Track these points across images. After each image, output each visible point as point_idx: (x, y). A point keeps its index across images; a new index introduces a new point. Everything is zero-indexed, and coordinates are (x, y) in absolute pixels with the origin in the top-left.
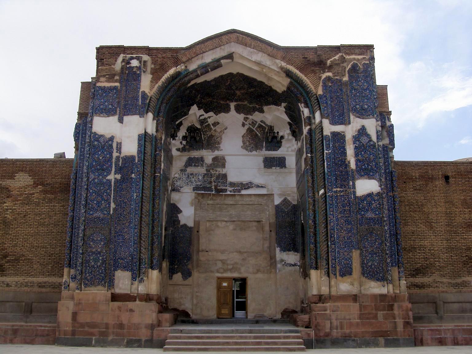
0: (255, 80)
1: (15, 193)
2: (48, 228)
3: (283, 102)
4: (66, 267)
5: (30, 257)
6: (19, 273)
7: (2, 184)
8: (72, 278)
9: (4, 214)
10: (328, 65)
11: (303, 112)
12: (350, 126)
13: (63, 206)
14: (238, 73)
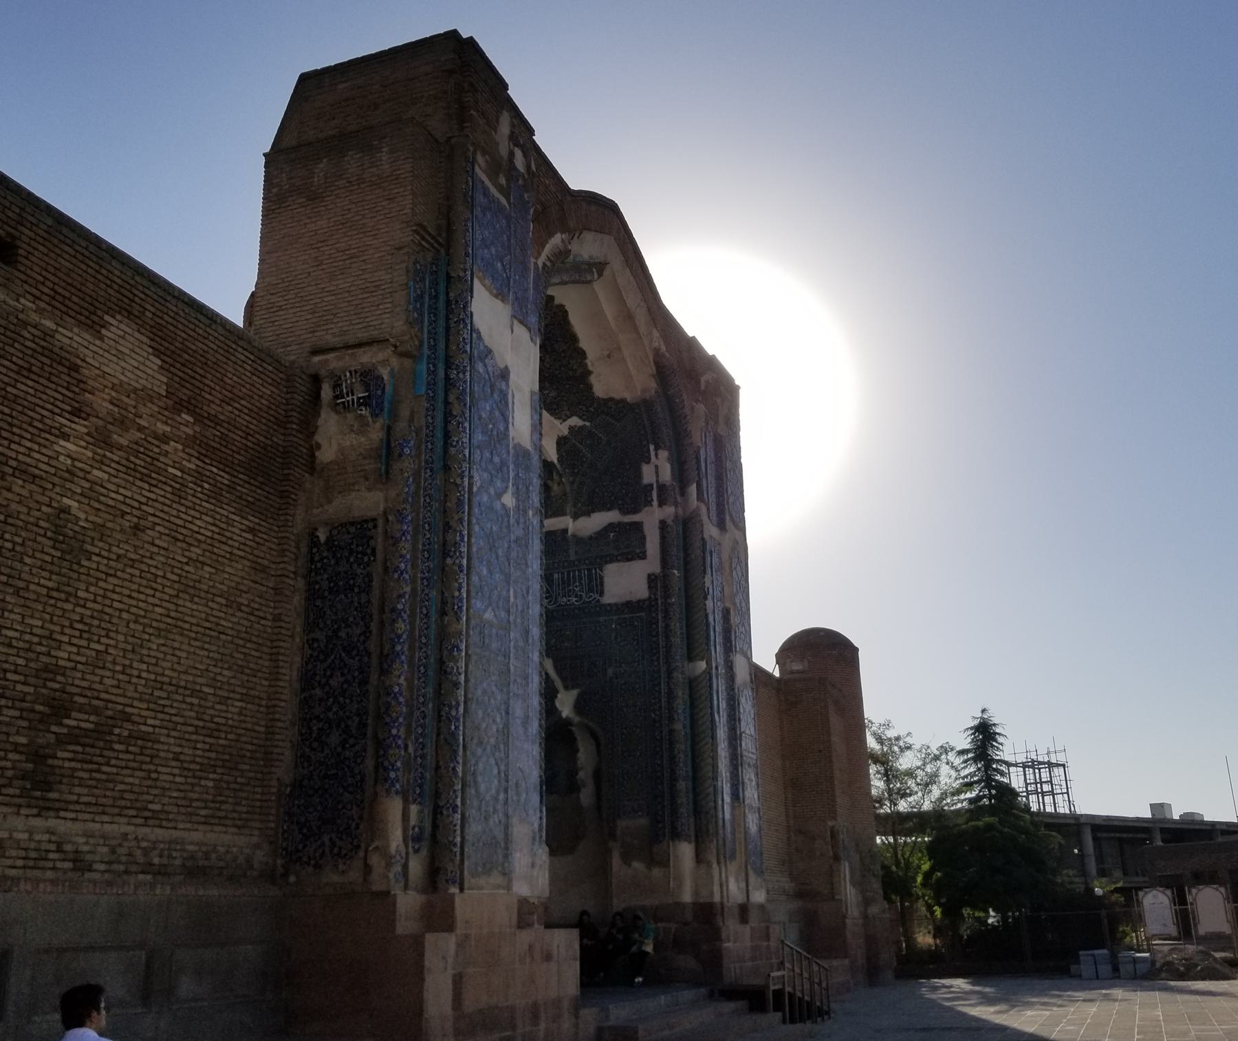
0: (574, 339)
1: (101, 403)
2: (209, 611)
3: (580, 418)
4: (397, 793)
5: (151, 730)
6: (110, 802)
7: (57, 336)
8: (413, 840)
9: (58, 489)
10: (703, 387)
11: (657, 467)
12: (727, 536)
13: (251, 530)
14: (562, 307)
